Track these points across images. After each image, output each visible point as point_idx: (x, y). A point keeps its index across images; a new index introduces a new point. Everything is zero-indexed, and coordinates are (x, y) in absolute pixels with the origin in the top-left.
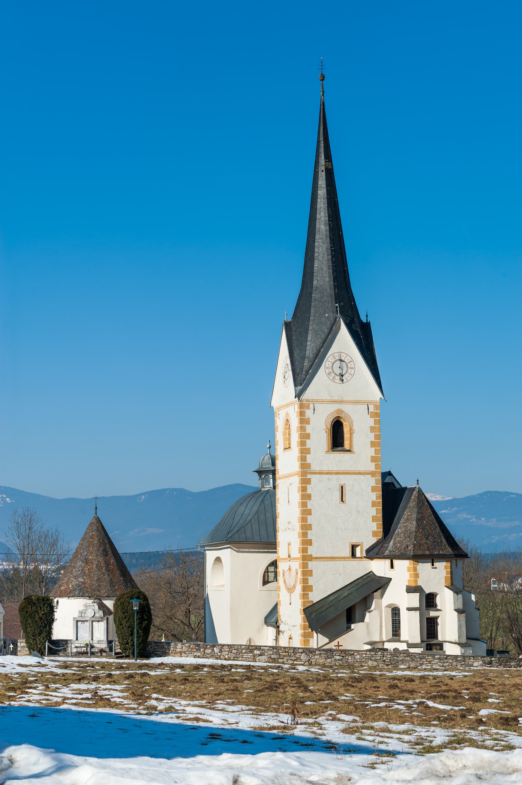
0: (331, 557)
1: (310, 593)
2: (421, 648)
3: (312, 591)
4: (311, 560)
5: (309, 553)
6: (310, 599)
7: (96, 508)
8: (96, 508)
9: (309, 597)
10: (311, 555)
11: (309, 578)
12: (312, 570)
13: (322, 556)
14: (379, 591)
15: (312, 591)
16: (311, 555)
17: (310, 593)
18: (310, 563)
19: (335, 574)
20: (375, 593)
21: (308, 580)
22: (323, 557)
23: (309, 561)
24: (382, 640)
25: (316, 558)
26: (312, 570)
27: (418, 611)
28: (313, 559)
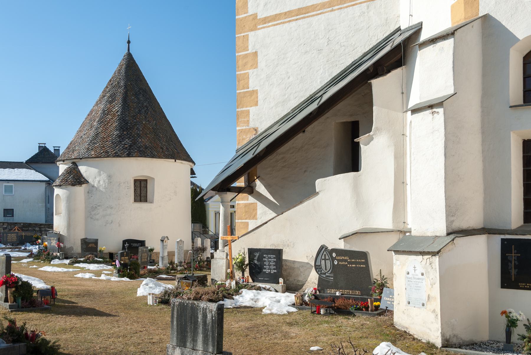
0: (299, 9)
1: (253, 110)
2: (434, 254)
3: (256, 104)
4: (254, 28)
5: (251, 12)
6: (252, 125)
7: (129, 42)
8: (129, 42)
9: (251, 120)
10: (255, 16)
11: (250, 71)
12: (256, 53)
13: (278, 12)
14: (396, 74)
15: (256, 104)
16: (255, 16)
17: (253, 110)
18: (251, 34)
19: (306, 52)
20: (376, 83)
21: (248, 78)
22: (280, 14)
23: (252, 30)
24: (401, 227)
25: (266, 20)
26: (256, 53)
27: (441, 110)
28: (259, 24)
